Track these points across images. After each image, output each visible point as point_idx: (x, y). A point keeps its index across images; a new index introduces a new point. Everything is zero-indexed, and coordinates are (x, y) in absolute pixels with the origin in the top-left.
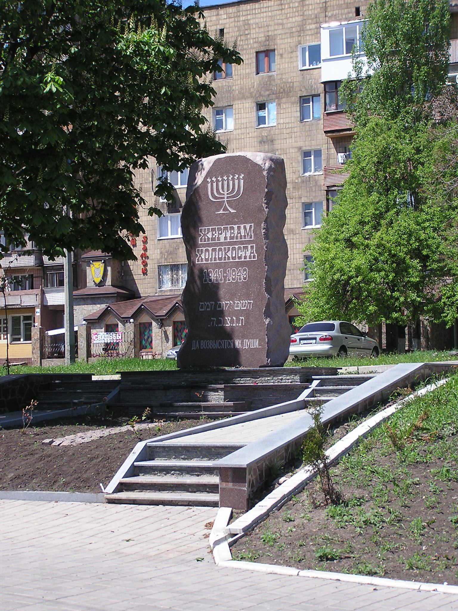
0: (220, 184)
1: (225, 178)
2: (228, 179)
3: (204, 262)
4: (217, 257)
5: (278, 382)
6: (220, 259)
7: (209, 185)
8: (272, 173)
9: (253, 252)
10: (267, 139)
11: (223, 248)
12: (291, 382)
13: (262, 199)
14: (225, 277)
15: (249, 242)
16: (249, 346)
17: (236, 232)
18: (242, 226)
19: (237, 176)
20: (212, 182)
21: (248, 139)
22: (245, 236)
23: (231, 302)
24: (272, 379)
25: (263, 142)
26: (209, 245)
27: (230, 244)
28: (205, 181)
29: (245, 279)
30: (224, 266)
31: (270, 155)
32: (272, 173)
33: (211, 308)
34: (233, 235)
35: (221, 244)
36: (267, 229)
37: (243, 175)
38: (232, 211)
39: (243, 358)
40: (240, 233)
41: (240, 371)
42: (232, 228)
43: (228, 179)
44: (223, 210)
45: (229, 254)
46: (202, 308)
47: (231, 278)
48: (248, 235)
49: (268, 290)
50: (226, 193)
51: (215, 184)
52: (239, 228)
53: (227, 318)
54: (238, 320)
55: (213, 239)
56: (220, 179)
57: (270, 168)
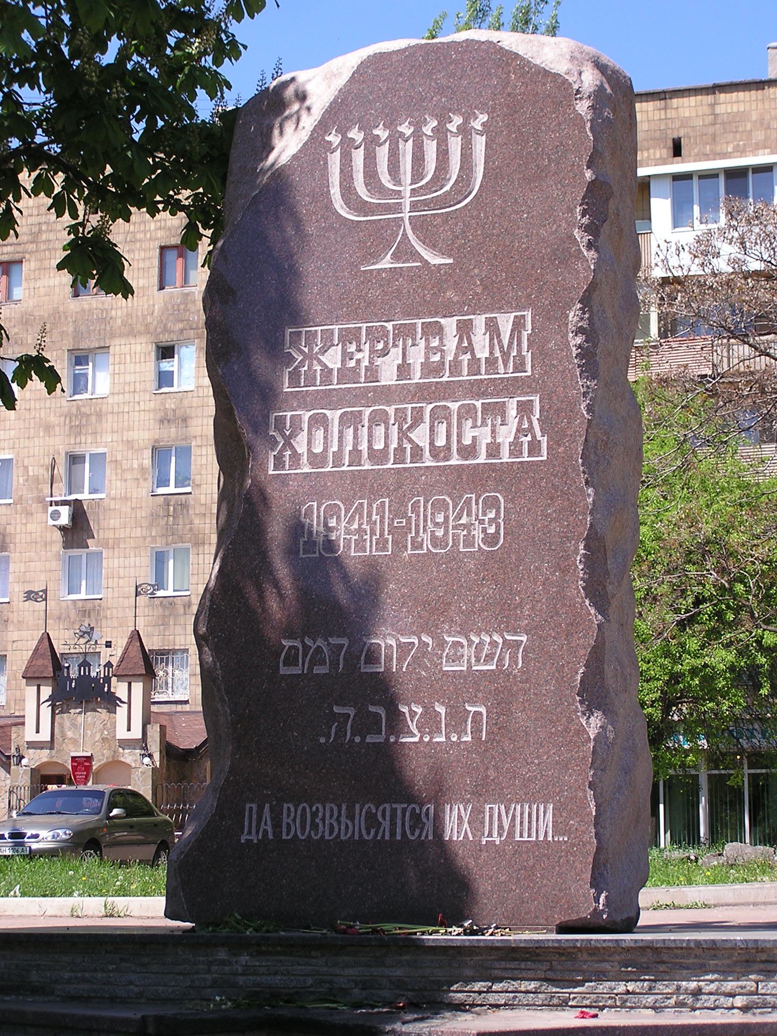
0: (383, 153)
1: (406, 129)
2: (418, 136)
3: (307, 470)
4: (364, 447)
5: (680, 1004)
6: (378, 456)
7: (335, 160)
8: (607, 113)
9: (531, 429)
10: (174, 416)
11: (391, 410)
12: (745, 1009)
13: (571, 210)
14: (400, 534)
15: (510, 387)
16: (511, 833)
17: (451, 344)
18: (479, 321)
19: (458, 120)
20: (347, 146)
21: (136, 414)
22: (491, 362)
23: (426, 639)
24: (650, 991)
25: (166, 422)
26: (328, 399)
27: (423, 393)
28: (316, 145)
29: (491, 540)
30: (396, 486)
31: (591, 49)
32: (607, 113)
33: (334, 664)
34: (436, 358)
35: (386, 394)
36: (589, 333)
37: (483, 118)
38: (435, 260)
39: (486, 884)
40: (470, 349)
41: (492, 949)
42: (439, 330)
43: (418, 136)
44: (396, 257)
45: (420, 436)
46: (291, 660)
47: (426, 538)
48: (506, 355)
49: (597, 591)
50: (407, 190)
51: (358, 157)
52: (465, 329)
53: (405, 709)
54: (457, 719)
55: (346, 374)
56: (381, 132)
57: (599, 92)
